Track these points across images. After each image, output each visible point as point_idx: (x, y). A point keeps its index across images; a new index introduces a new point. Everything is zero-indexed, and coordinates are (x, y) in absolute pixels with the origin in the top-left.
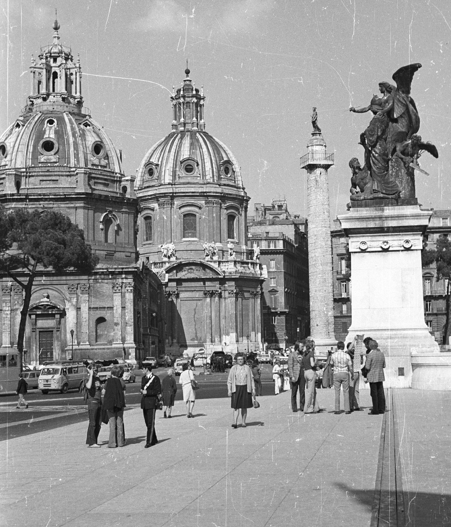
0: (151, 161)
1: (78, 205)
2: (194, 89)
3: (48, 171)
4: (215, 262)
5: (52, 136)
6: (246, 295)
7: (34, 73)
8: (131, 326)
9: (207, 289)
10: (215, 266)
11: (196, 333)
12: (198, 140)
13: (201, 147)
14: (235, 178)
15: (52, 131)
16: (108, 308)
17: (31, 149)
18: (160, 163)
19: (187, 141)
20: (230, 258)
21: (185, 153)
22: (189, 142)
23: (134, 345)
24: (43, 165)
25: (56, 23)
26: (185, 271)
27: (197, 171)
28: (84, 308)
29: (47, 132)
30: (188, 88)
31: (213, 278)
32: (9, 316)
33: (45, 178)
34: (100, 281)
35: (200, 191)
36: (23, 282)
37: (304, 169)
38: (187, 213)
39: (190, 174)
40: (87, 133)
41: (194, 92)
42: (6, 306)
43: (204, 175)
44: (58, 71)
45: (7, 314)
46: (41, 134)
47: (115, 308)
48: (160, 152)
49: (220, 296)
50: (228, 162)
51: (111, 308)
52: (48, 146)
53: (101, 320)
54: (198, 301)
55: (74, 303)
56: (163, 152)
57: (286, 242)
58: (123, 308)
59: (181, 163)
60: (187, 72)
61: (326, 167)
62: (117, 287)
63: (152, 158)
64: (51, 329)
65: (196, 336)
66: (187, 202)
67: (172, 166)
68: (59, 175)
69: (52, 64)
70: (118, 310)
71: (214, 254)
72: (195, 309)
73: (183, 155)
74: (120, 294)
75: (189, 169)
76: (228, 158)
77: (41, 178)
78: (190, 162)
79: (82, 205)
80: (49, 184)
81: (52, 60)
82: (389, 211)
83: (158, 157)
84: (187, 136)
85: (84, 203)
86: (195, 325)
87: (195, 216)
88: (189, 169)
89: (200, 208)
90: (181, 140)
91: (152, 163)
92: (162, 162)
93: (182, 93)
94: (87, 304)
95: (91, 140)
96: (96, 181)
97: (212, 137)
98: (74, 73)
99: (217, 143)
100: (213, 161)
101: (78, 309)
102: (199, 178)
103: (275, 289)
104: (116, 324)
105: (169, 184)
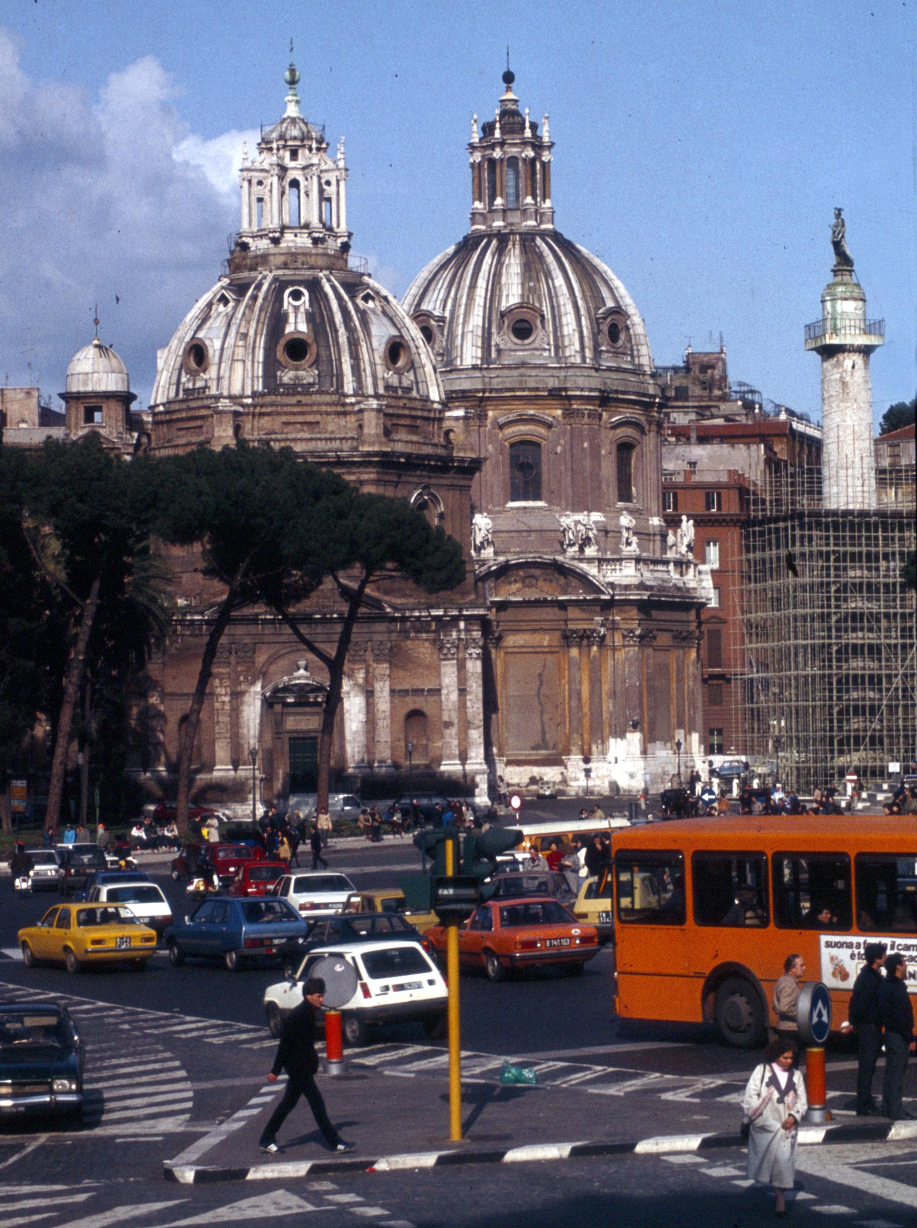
0: (424, 307)
1: (365, 477)
2: (527, 124)
3: (299, 403)
4: (590, 560)
5: (303, 327)
6: (664, 639)
7: (250, 182)
8: (478, 727)
9: (570, 627)
10: (592, 570)
11: (544, 733)
12: (541, 257)
13: (548, 275)
14: (632, 350)
15: (302, 317)
16: (430, 690)
17: (260, 355)
18: (447, 314)
20: (627, 551)
21: (512, 294)
22: (518, 261)
23: (485, 767)
26: (516, 581)
27: (542, 337)
28: (382, 690)
29: (291, 319)
31: (585, 600)
32: (227, 707)
33: (292, 419)
34: (412, 635)
35: (550, 386)
37: (814, 353)
38: (517, 439)
39: (527, 342)
41: (528, 133)
42: (221, 686)
43: (559, 347)
44: (301, 179)
45: (224, 702)
46: (278, 320)
47: (444, 692)
48: (445, 285)
50: (618, 311)
51: (437, 692)
52: (297, 349)
53: (416, 715)
54: (549, 656)
55: (361, 681)
57: (742, 489)
58: (462, 692)
59: (503, 315)
60: (509, 78)
61: (866, 351)
62: (449, 649)
63: (426, 300)
64: (312, 735)
65: (544, 739)
66: (520, 412)
67: (480, 324)
68: (320, 413)
69: (288, 162)
70: (450, 696)
71: (587, 541)
72: (540, 675)
73: (507, 296)
74: (455, 662)
75: (523, 330)
76: (617, 301)
77: (284, 419)
78: (527, 314)
79: (373, 476)
80: (298, 432)
81: (287, 154)
83: (441, 296)
84: (514, 245)
85: (378, 473)
86: (542, 713)
88: (523, 330)
89: (549, 426)
90: (500, 255)
91: (428, 315)
92: (453, 312)
93: (497, 134)
94: (387, 683)
96: (395, 422)
97: (573, 247)
98: (334, 182)
99: (587, 260)
100: (583, 311)
101: (369, 694)
102: (546, 354)
103: (720, 614)
104: (448, 725)
105: (475, 367)
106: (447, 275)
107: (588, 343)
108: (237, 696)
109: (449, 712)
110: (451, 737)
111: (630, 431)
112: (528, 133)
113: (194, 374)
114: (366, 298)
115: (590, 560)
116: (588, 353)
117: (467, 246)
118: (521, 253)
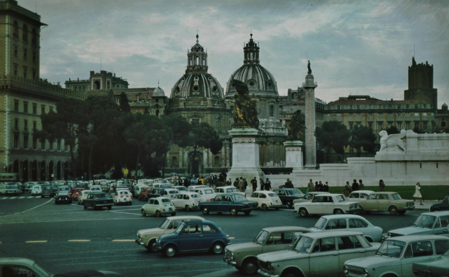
4: (263, 128)
5: (197, 84)
12: (256, 70)
13: (257, 73)
17: (189, 89)
20: (271, 126)
27: (255, 86)
40: (211, 82)
43: (259, 87)
46: (192, 82)
49: (266, 144)
52: (196, 88)
58: (226, 153)
59: (248, 81)
60: (251, 35)
71: (263, 124)
78: (252, 81)
82: (294, 142)
95: (212, 85)
104: (223, 159)
107: (264, 86)
108: (183, 153)
109: (223, 157)
110: (223, 161)
111: (272, 103)
112: (255, 46)
113: (177, 93)
114: (210, 79)
115: (263, 128)
116: (264, 88)
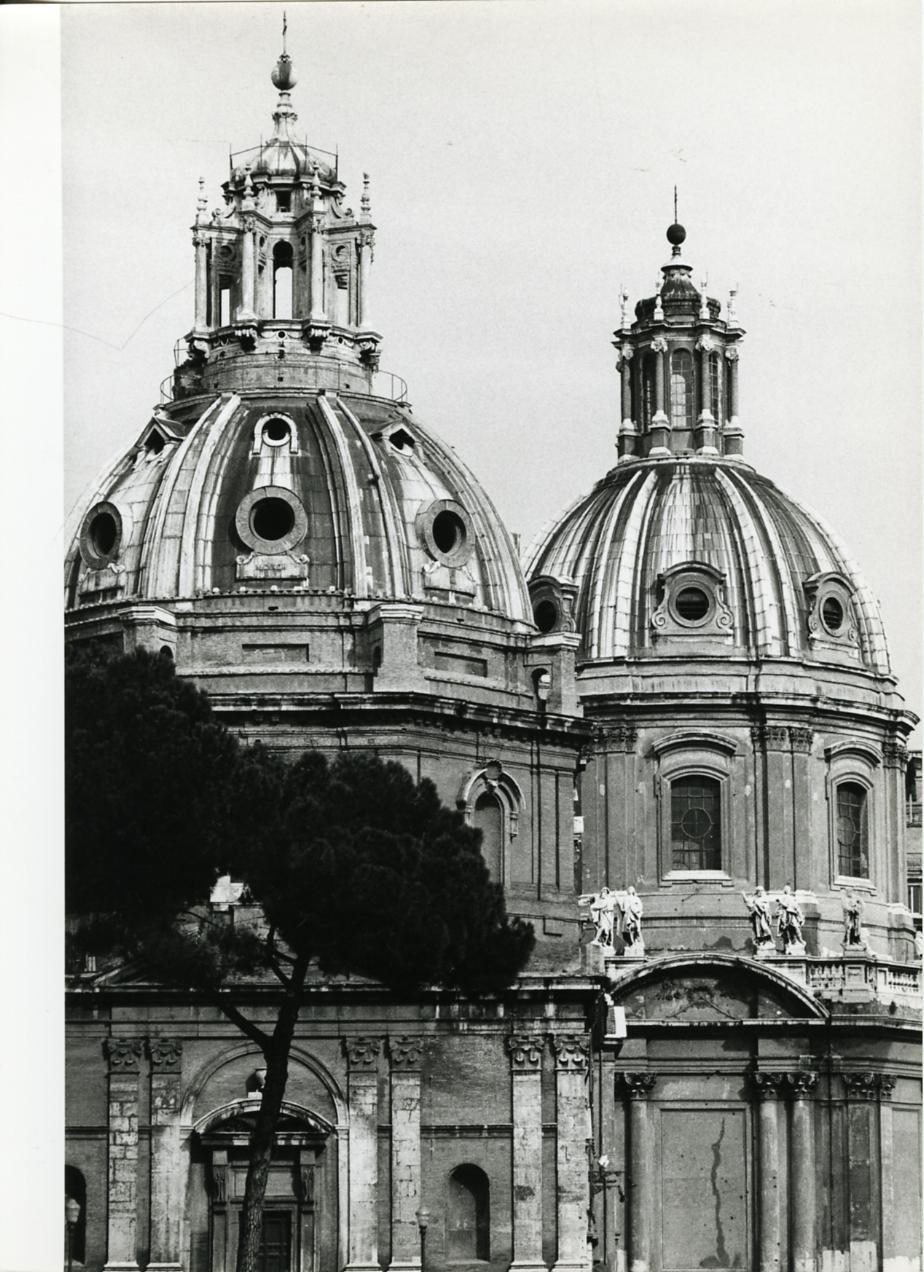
0: (544, 572)
2: (704, 301)
3: (272, 612)
4: (794, 963)
5: (284, 479)
10: (796, 978)
11: (721, 1239)
13: (733, 521)
15: (283, 465)
16: (492, 1129)
18: (579, 582)
19: (681, 501)
21: (677, 548)
22: (687, 501)
24: (251, 591)
25: (285, 63)
26: (678, 996)
27: (724, 616)
28: (406, 1128)
29: (265, 467)
30: (678, 295)
31: (785, 1025)
33: (259, 638)
34: (463, 1026)
35: (734, 690)
36: (261, 1027)
38: (684, 773)
39: (697, 623)
40: (407, 470)
41: (705, 313)
43: (749, 630)
46: (240, 474)
47: (518, 1132)
48: (578, 539)
51: (506, 1131)
52: (274, 519)
54: (729, 1116)
55: (368, 1110)
56: (592, 539)
58: (551, 1132)
59: (661, 581)
60: (676, 235)
62: (527, 1053)
63: (548, 563)
65: (721, 1250)
66: (687, 730)
68: (311, 629)
70: (529, 1141)
71: (788, 934)
72: (716, 1147)
73: (670, 552)
74: (538, 1077)
75: (694, 606)
77: (246, 638)
80: (273, 660)
84: (681, 479)
86: (718, 1207)
87: (714, 785)
90: (660, 493)
91: (551, 583)
92: (589, 579)
93: (659, 314)
94: (416, 1114)
95: (422, 493)
96: (441, 649)
100: (785, 577)
101: (384, 1132)
102: (729, 641)
104: (524, 1193)
105: (618, 661)
106: (582, 523)
107: (794, 626)
108: (149, 1133)
109: (528, 1173)
110: (531, 1216)
111: (858, 766)
112: (705, 313)
114: (400, 439)
115: (794, 963)
116: (794, 641)
117: (610, 485)
118: (693, 490)
